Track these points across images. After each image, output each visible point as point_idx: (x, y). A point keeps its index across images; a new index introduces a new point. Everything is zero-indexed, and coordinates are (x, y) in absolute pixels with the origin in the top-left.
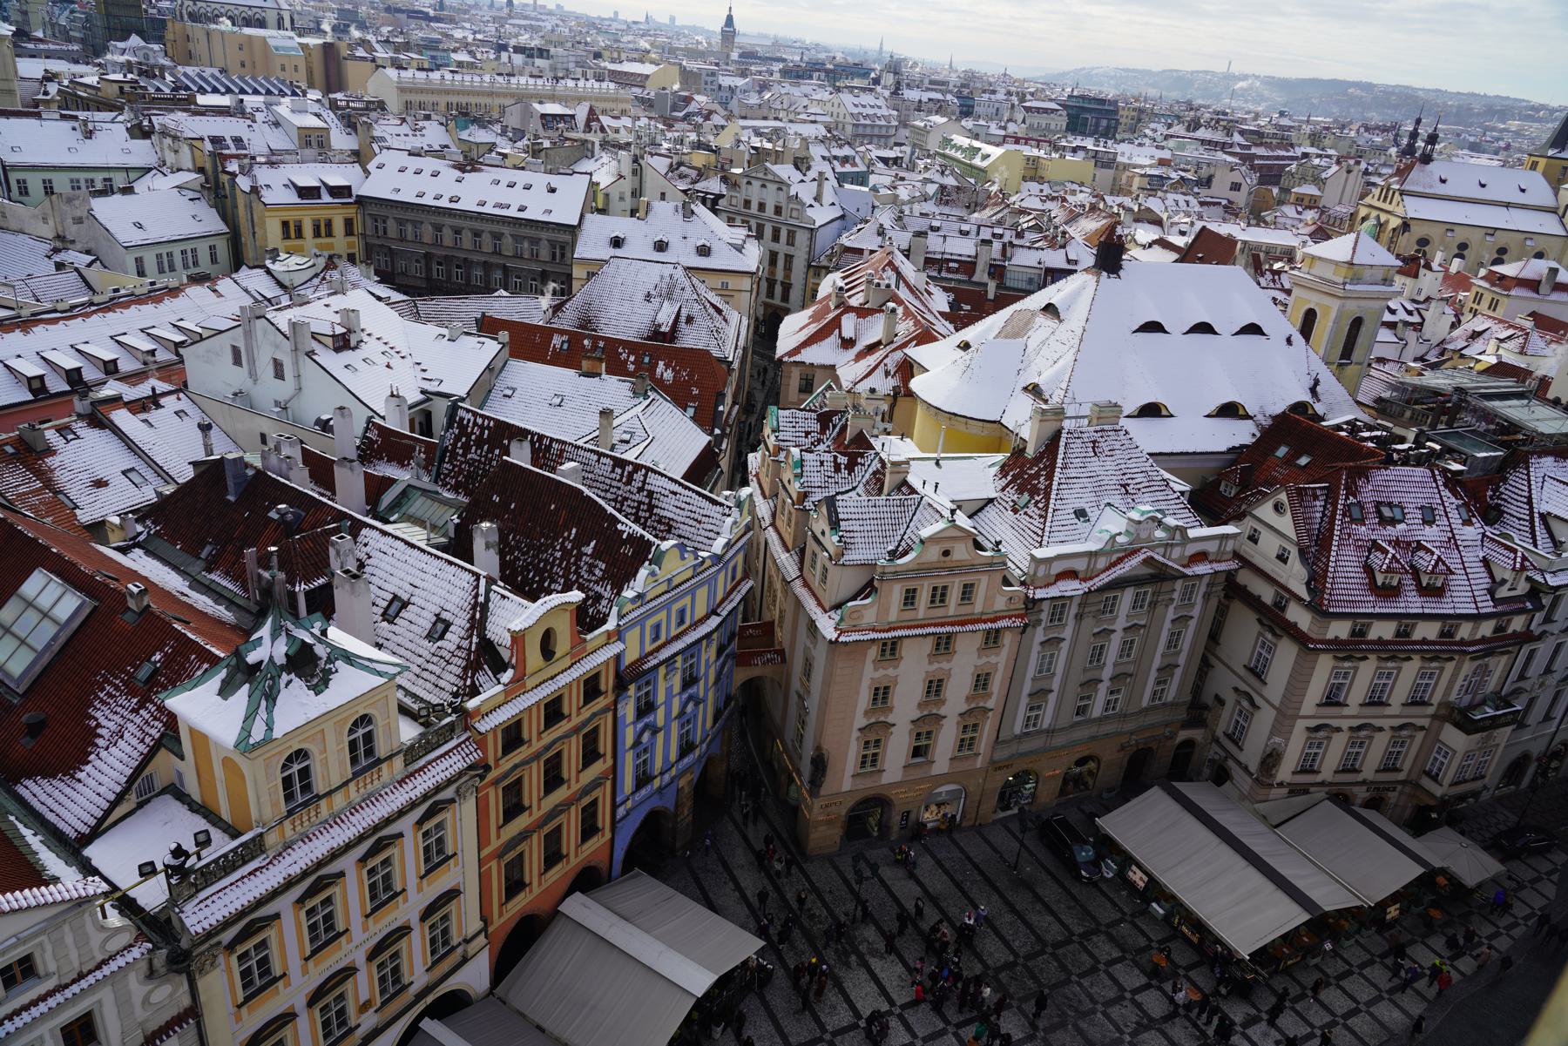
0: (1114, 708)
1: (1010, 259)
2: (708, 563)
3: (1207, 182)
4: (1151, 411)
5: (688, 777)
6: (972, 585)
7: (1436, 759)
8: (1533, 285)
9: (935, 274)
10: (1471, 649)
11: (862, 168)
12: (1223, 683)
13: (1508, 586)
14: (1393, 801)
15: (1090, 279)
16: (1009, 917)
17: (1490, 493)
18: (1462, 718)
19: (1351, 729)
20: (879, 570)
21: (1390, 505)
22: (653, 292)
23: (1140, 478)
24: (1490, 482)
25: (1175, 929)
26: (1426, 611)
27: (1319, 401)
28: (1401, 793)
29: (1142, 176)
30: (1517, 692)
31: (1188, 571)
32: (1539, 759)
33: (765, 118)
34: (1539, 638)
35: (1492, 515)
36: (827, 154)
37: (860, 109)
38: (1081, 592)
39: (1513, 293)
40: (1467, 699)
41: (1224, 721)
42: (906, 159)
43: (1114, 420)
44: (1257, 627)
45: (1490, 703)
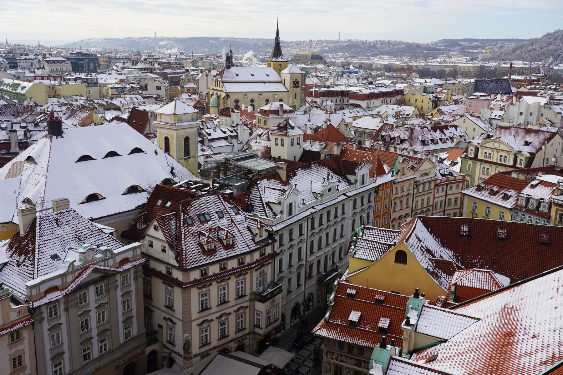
0: (105, 349)
1: (30, 138)
3: (145, 88)
4: (93, 198)
7: (257, 318)
8: (276, 112)
10: (252, 266)
12: (159, 317)
13: (258, 236)
14: (248, 344)
15: (47, 140)
17: (246, 199)
18: (263, 299)
21: (204, 214)
23: (86, 231)
24: (245, 195)
26: (229, 256)
27: (176, 176)
28: (250, 339)
29: (112, 88)
31: (120, 270)
32: (303, 304)
34: (279, 254)
35: (249, 208)
38: (61, 296)
39: (270, 117)
40: (261, 289)
41: (165, 337)
43: (66, 207)
44: (164, 286)
45: (271, 287)
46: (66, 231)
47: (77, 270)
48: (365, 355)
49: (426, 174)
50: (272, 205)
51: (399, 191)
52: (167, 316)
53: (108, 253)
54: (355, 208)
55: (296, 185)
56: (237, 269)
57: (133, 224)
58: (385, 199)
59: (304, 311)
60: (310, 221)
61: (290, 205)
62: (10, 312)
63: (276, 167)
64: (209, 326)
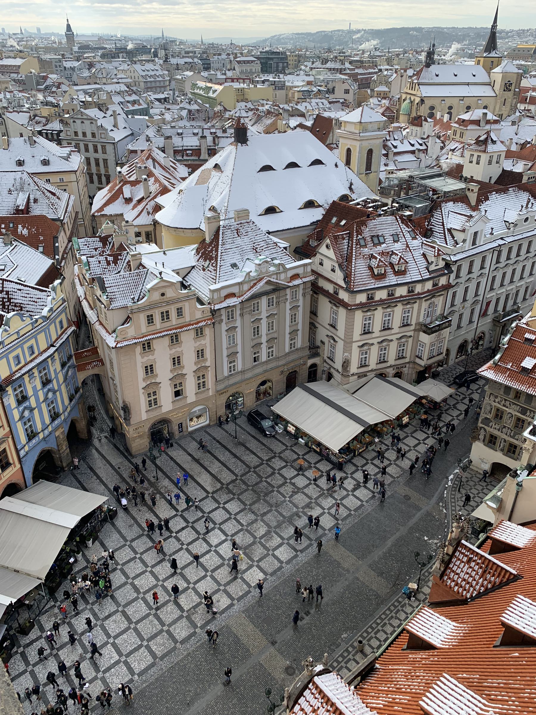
0: (272, 355)
2: (40, 321)
3: (332, 91)
4: (271, 210)
5: (61, 430)
8: (477, 123)
9: (180, 158)
11: (145, 106)
12: (322, 334)
13: (434, 264)
14: (406, 372)
15: (233, 148)
16: (234, 460)
17: (426, 223)
18: (428, 330)
20: (130, 308)
21: (378, 236)
22: (12, 189)
23: (262, 244)
24: (426, 218)
25: (310, 448)
26: (399, 282)
27: (354, 193)
29: (298, 91)
32: (472, 342)
33: (89, 84)
35: (427, 233)
36: (122, 100)
37: (146, 73)
39: (469, 128)
40: (428, 320)
41: (326, 352)
42: (171, 98)
43: (246, 217)
44: (330, 305)
46: (244, 242)
47: (253, 280)
50: (453, 231)
52: (330, 334)
55: (486, 211)
56: (405, 296)
59: (472, 349)
60: (496, 253)
61: (476, 233)
63: (465, 188)
64: (369, 349)
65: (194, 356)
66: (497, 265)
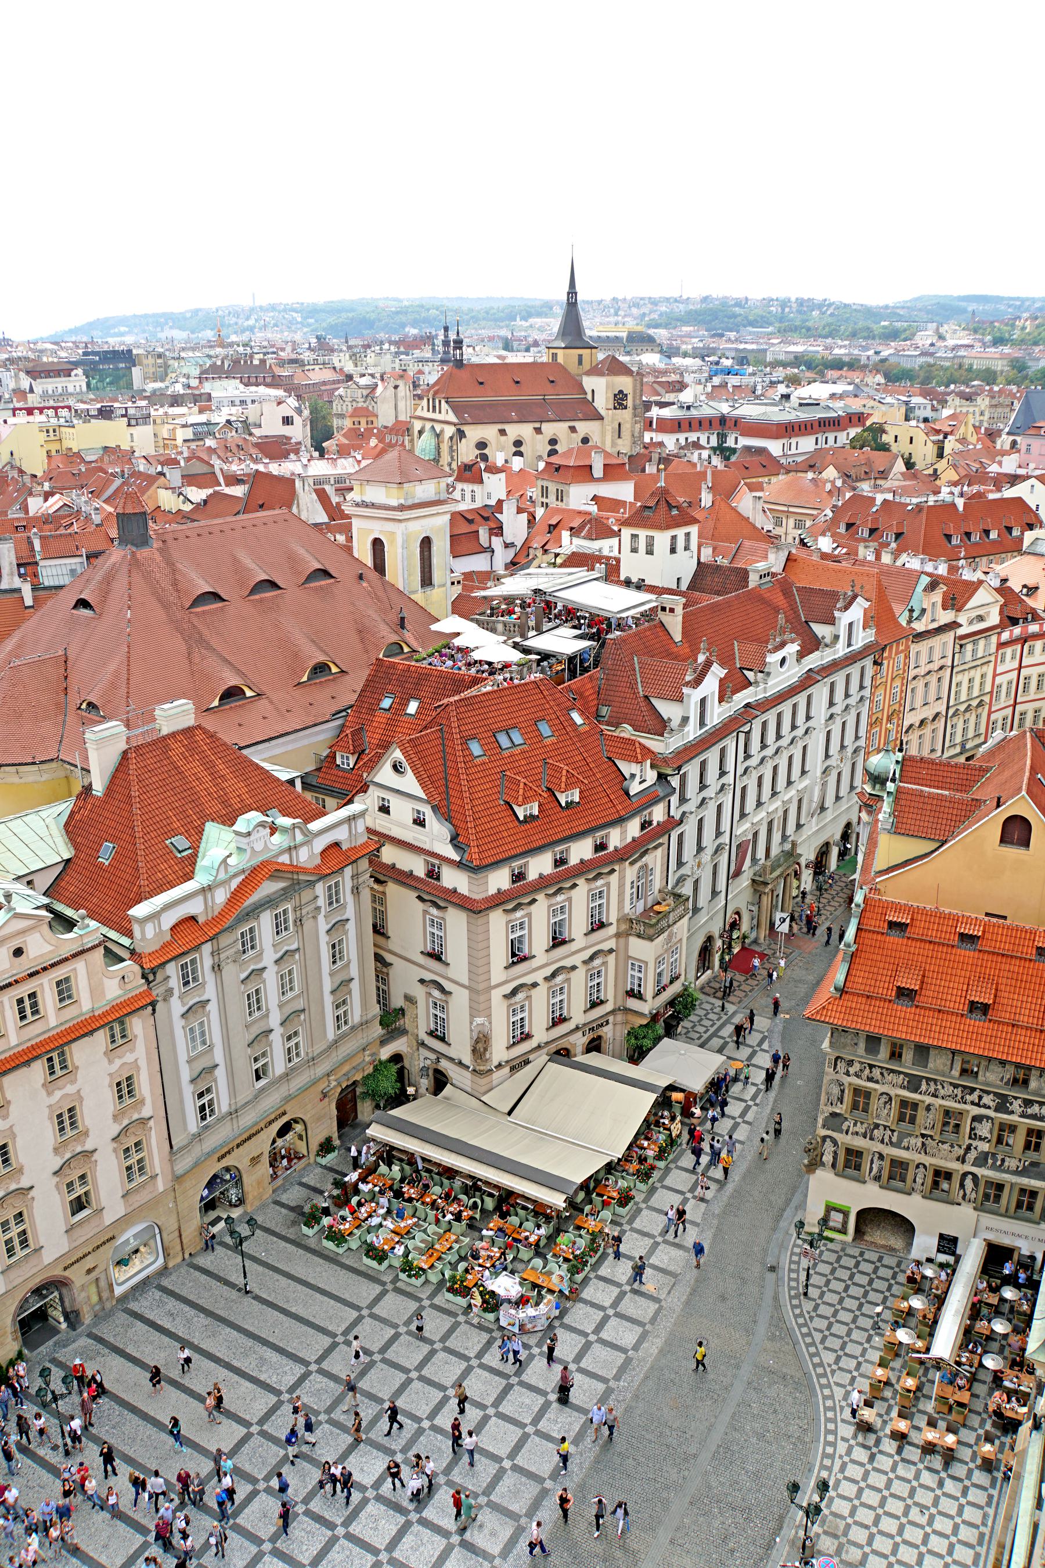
0: (297, 1055)
6: (67, 979)
7: (633, 976)
13: (638, 779)
14: (610, 1035)
19: (546, 979)
30: (681, 880)
32: (721, 936)
34: (681, 821)
41: (421, 1022)
44: (420, 906)
47: (235, 876)
48: (931, 1065)
49: (981, 618)
51: (924, 659)
52: (428, 976)
53: (297, 831)
54: (831, 704)
57: (325, 754)
58: (893, 679)
62: (105, 980)
65: (109, 1095)
66: (748, 763)
